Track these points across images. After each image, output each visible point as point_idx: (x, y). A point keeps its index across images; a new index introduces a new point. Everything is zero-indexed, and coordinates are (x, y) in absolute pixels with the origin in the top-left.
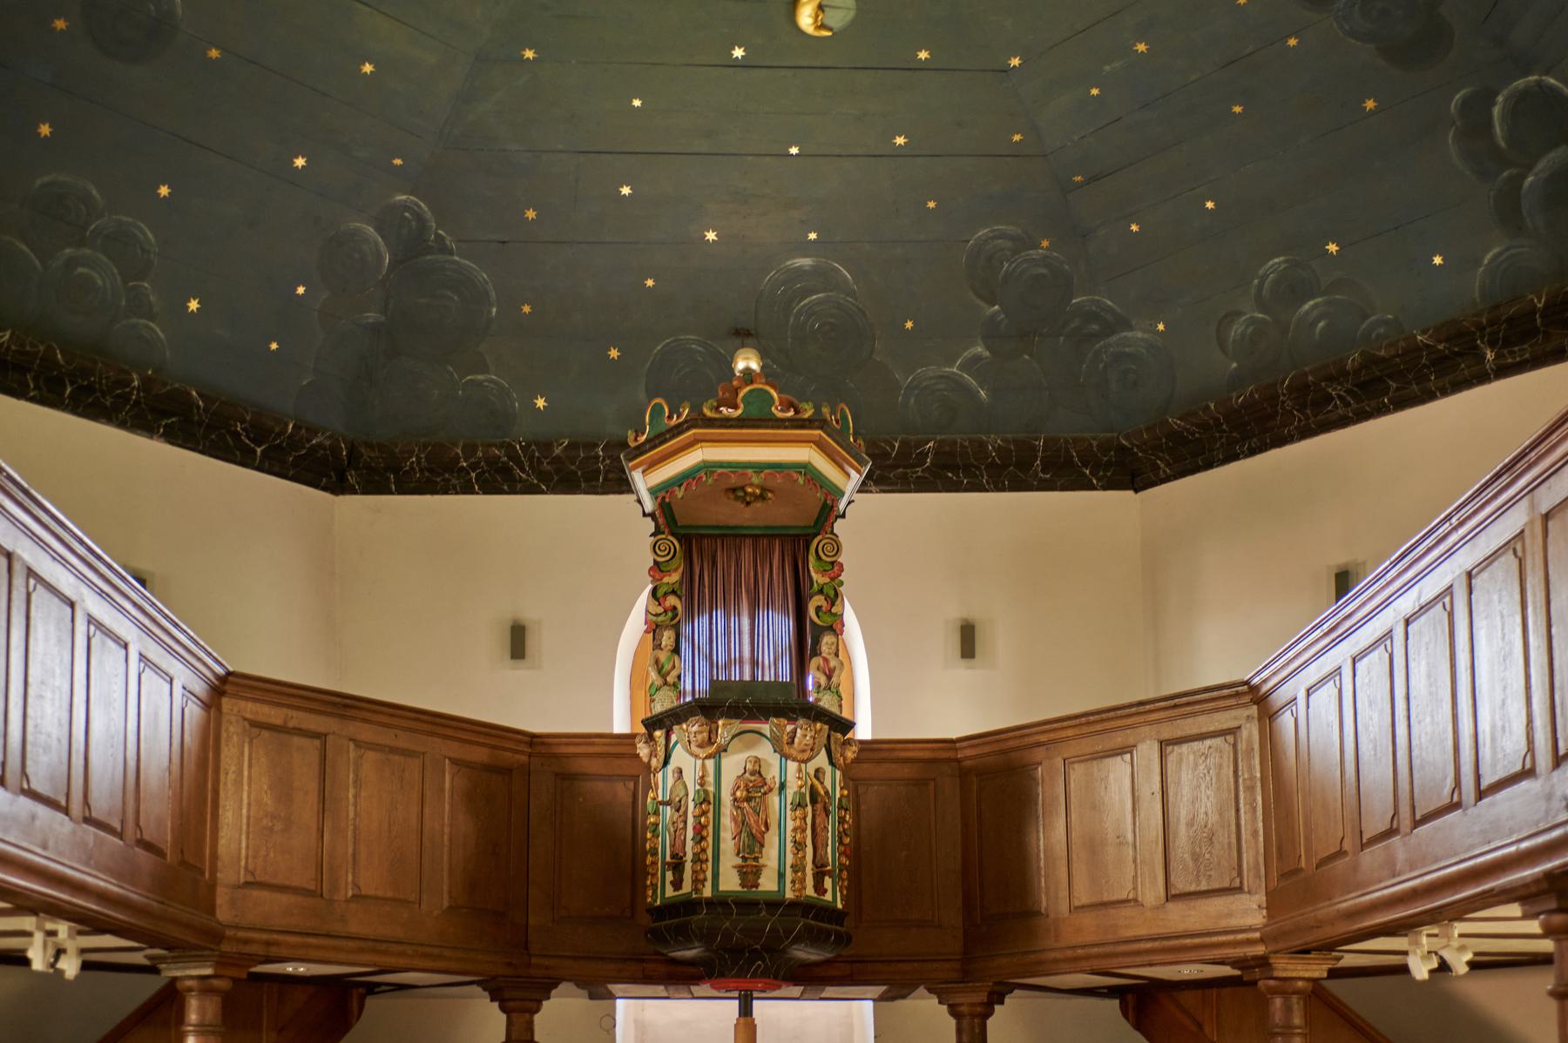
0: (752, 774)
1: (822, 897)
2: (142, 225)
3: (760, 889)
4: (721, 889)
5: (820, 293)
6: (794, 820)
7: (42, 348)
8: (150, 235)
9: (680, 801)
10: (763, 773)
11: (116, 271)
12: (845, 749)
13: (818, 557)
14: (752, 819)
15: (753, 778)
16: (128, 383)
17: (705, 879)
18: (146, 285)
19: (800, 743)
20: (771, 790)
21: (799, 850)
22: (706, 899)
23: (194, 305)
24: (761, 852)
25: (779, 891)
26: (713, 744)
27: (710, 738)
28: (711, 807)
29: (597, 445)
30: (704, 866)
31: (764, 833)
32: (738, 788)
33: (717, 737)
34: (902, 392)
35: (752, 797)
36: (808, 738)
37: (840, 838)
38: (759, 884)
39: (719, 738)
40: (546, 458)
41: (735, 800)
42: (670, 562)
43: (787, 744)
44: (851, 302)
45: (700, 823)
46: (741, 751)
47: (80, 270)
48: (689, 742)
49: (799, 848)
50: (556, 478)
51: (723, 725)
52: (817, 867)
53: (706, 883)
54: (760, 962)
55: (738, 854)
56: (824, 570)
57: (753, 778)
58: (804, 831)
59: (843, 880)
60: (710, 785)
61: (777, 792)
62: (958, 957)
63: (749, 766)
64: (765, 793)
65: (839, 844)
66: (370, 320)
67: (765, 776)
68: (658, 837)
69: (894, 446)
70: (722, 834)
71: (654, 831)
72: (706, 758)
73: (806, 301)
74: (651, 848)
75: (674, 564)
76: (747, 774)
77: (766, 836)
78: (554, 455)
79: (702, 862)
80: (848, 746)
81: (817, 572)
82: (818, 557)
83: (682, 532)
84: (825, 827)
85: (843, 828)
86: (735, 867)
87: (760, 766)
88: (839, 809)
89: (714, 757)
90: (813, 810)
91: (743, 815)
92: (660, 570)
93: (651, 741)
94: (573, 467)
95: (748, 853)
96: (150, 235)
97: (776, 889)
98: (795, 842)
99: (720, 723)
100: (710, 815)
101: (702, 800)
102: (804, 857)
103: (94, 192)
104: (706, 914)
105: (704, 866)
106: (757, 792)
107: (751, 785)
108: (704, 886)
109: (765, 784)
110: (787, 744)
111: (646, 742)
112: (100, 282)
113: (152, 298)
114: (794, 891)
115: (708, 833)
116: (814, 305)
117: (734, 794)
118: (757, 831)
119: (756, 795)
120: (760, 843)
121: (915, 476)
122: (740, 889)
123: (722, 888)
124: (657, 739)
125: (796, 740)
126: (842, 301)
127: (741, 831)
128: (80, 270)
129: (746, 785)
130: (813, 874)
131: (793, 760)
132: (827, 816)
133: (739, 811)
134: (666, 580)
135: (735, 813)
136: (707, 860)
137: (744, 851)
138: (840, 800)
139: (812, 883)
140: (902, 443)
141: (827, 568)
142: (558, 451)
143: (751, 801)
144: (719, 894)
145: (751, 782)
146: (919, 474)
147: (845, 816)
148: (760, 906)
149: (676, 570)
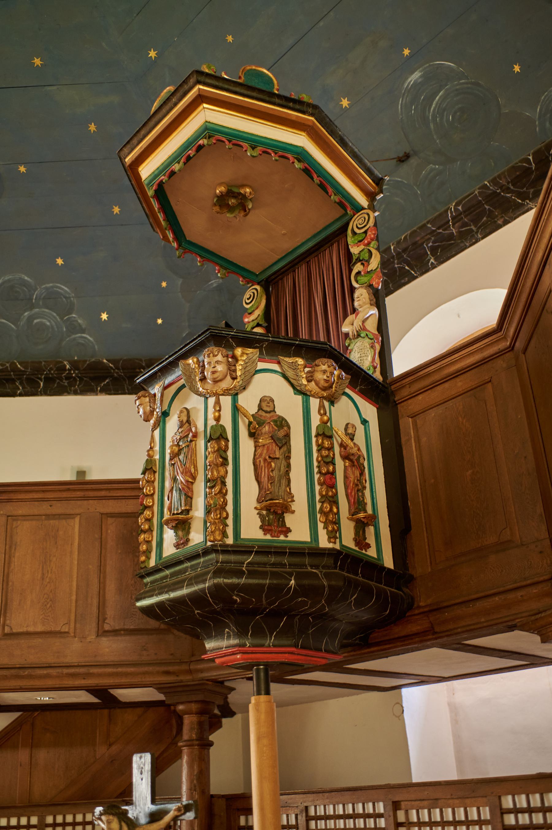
2: (59, 285)
5: (440, 92)
7: (8, 365)
8: (66, 289)
11: (55, 314)
16: (64, 368)
18: (74, 316)
23: (104, 316)
44: (467, 83)
47: (35, 321)
62: (546, 577)
66: (215, 285)
69: (529, 159)
73: (434, 105)
96: (66, 289)
103: (26, 278)
112: (48, 323)
113: (79, 321)
116: (440, 104)
126: (458, 87)
128: (35, 321)
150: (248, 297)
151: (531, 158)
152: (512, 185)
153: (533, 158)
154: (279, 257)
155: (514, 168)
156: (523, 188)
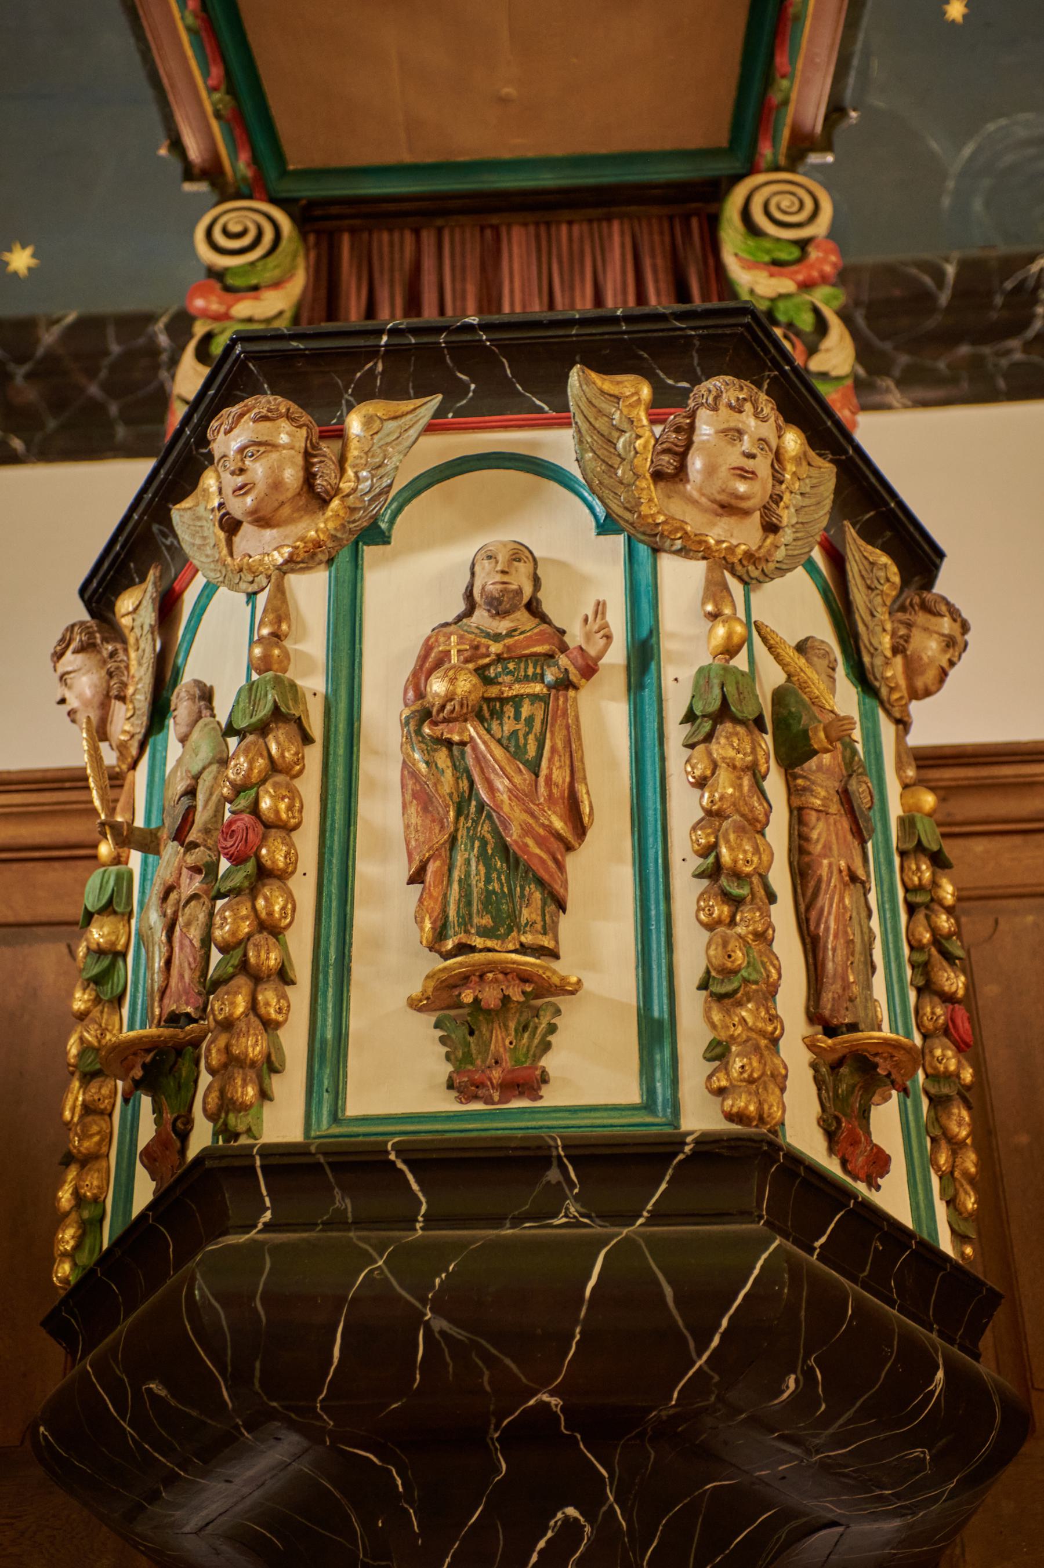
0: (499, 607)
1: (861, 1187)
3: (552, 1097)
4: (353, 1108)
6: (701, 783)
9: (191, 792)
10: (548, 607)
12: (909, 625)
13: (752, 229)
14: (501, 784)
15: (503, 626)
17: (272, 1065)
19: (711, 470)
20: (589, 670)
21: (736, 902)
22: (270, 1151)
24: (550, 928)
25: (649, 1105)
26: (323, 502)
27: (309, 478)
28: (313, 755)
29: (150, 318)
30: (268, 996)
31: (569, 848)
32: (438, 664)
33: (342, 471)
34: (951, 184)
35: (503, 701)
36: (747, 445)
37: (923, 968)
38: (545, 1079)
39: (350, 473)
40: (20, 360)
41: (425, 715)
42: (260, 264)
43: (658, 476)
45: (254, 808)
46: (449, 537)
48: (231, 526)
49: (736, 891)
50: (52, 424)
51: (368, 422)
52: (831, 1031)
53: (277, 1085)
54: (571, 1511)
55: (440, 933)
56: (776, 263)
57: (503, 626)
58: (756, 826)
59: (956, 1146)
60: (306, 674)
61: (619, 681)
63: (488, 580)
64: (565, 684)
65: (919, 991)
67: (558, 624)
68: (120, 999)
70: (365, 868)
71: (98, 981)
72: (293, 564)
74: (86, 1049)
75: (270, 272)
76: (481, 617)
77: (571, 861)
78: (40, 352)
79: (257, 978)
80: (921, 618)
81: (750, 265)
82: (752, 229)
83: (307, 191)
84: (854, 878)
85: (934, 930)
86: (416, 1005)
87: (536, 581)
88: (903, 854)
89: (330, 561)
90: (792, 791)
91: (461, 771)
92: (228, 289)
93: (106, 640)
94: (94, 390)
95: (484, 932)
97: (634, 1096)
98: (714, 872)
99: (355, 424)
100: (309, 786)
101: (264, 711)
102: (764, 937)
104: (268, 1227)
105: (268, 996)
106: (527, 679)
107: (495, 648)
108: (264, 1095)
109: (564, 648)
110: (658, 476)
111: (81, 650)
114: (721, 1092)
115: (292, 859)
117: (420, 695)
118: (527, 831)
119: (518, 689)
120: (541, 883)
121: (1004, 362)
122: (448, 1104)
123: (353, 1108)
124: (126, 622)
125: (696, 463)
127: (453, 840)
129: (474, 652)
130: (814, 1066)
131: (684, 552)
132: (863, 842)
133: (442, 757)
134: (243, 308)
135: (423, 767)
136: (284, 976)
137: (465, 922)
138: (907, 823)
139: (815, 1109)
140: (966, 266)
141: (783, 256)
142: (49, 338)
143: (497, 715)
144: (336, 1130)
145: (497, 637)
146: (1018, 356)
147: (935, 884)
148: (553, 1175)
149: (276, 285)
150: (235, 228)
151: (950, 270)
152: (868, 318)
153: (958, 275)
154: (407, 158)
155: (890, 272)
156: (883, 338)
